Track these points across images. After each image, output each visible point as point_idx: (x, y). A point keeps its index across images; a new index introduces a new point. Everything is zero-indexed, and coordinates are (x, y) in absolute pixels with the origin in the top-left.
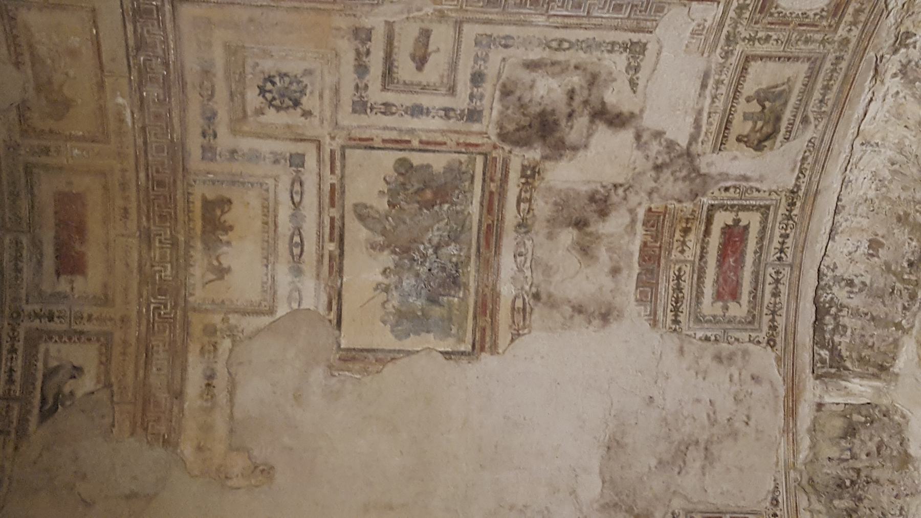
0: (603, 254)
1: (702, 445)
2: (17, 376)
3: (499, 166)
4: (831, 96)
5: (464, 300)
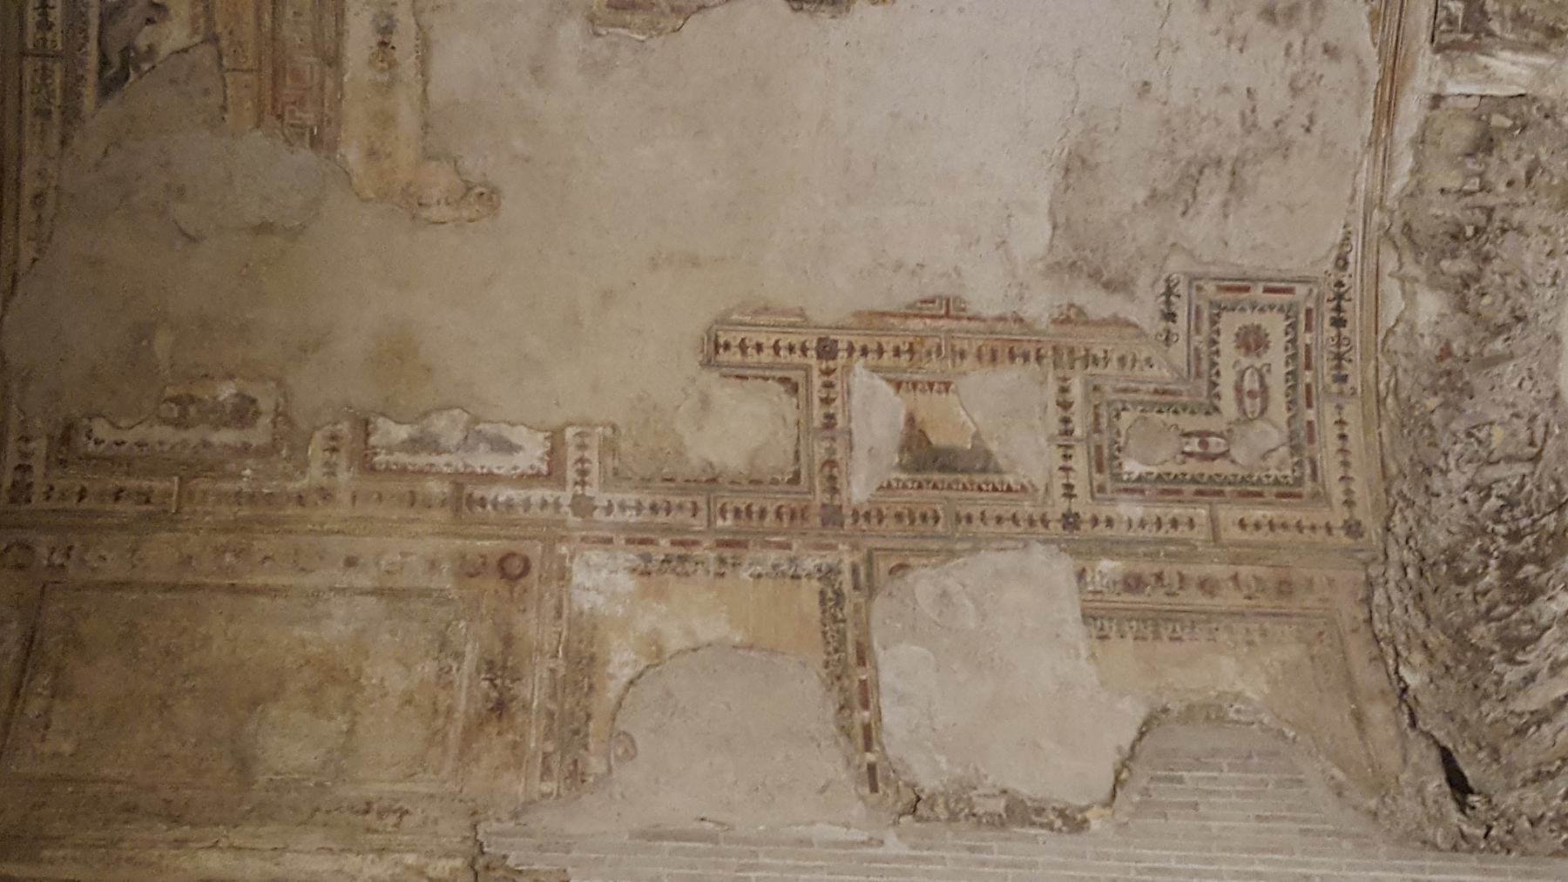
1: (1228, 167)
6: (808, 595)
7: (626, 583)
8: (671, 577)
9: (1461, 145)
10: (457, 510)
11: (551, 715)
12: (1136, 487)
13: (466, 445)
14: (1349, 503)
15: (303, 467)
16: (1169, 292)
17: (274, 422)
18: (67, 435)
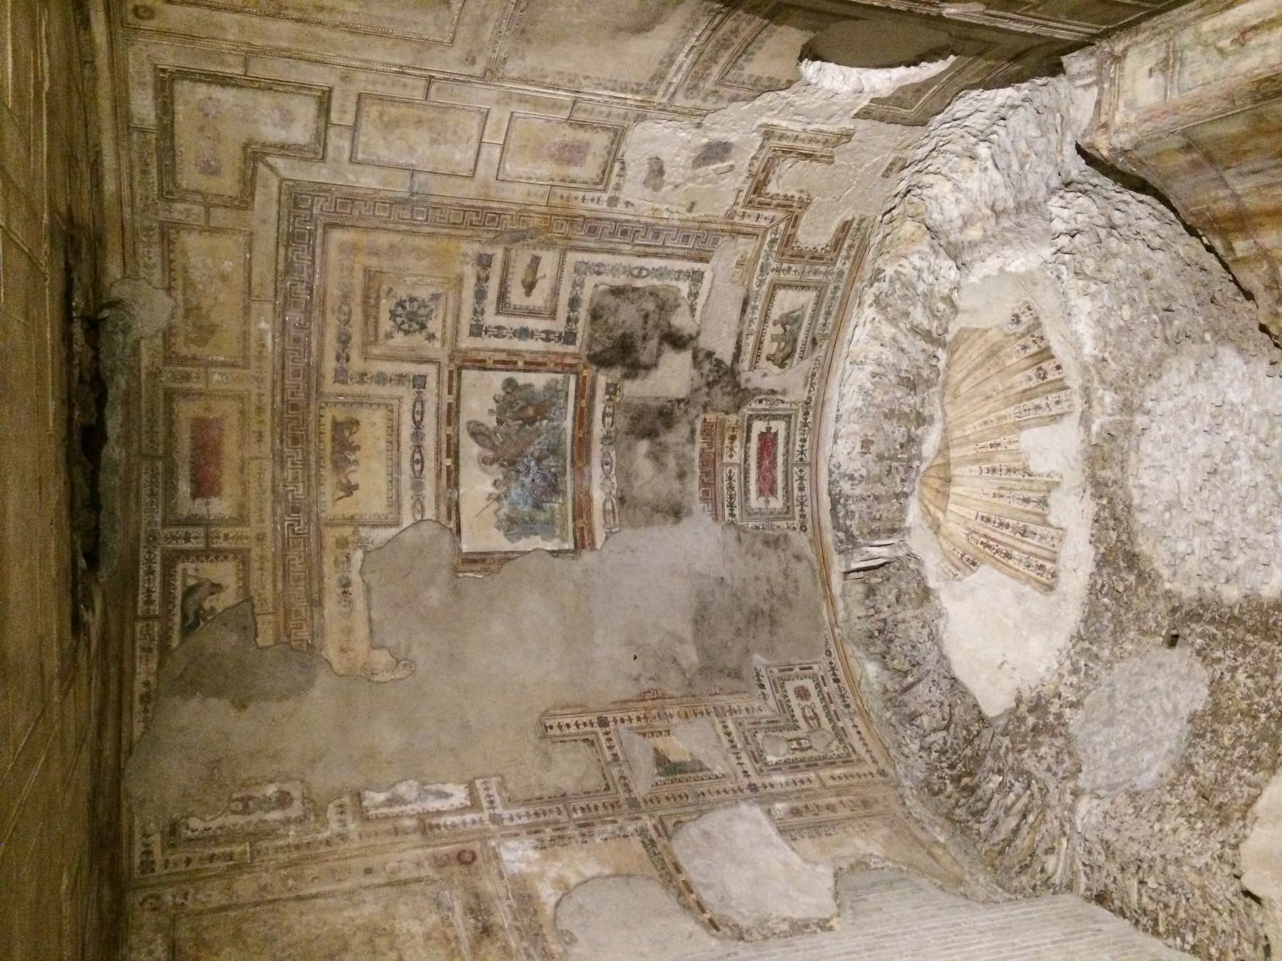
0: (671, 462)
2: (156, 596)
3: (588, 384)
4: (831, 320)
5: (564, 504)
6: (636, 844)
7: (534, 855)
8: (559, 848)
9: (860, 596)
10: (424, 832)
11: (518, 929)
12: (777, 768)
13: (420, 797)
14: (875, 762)
15: (326, 824)
16: (758, 675)
17: (303, 803)
18: (174, 829)
